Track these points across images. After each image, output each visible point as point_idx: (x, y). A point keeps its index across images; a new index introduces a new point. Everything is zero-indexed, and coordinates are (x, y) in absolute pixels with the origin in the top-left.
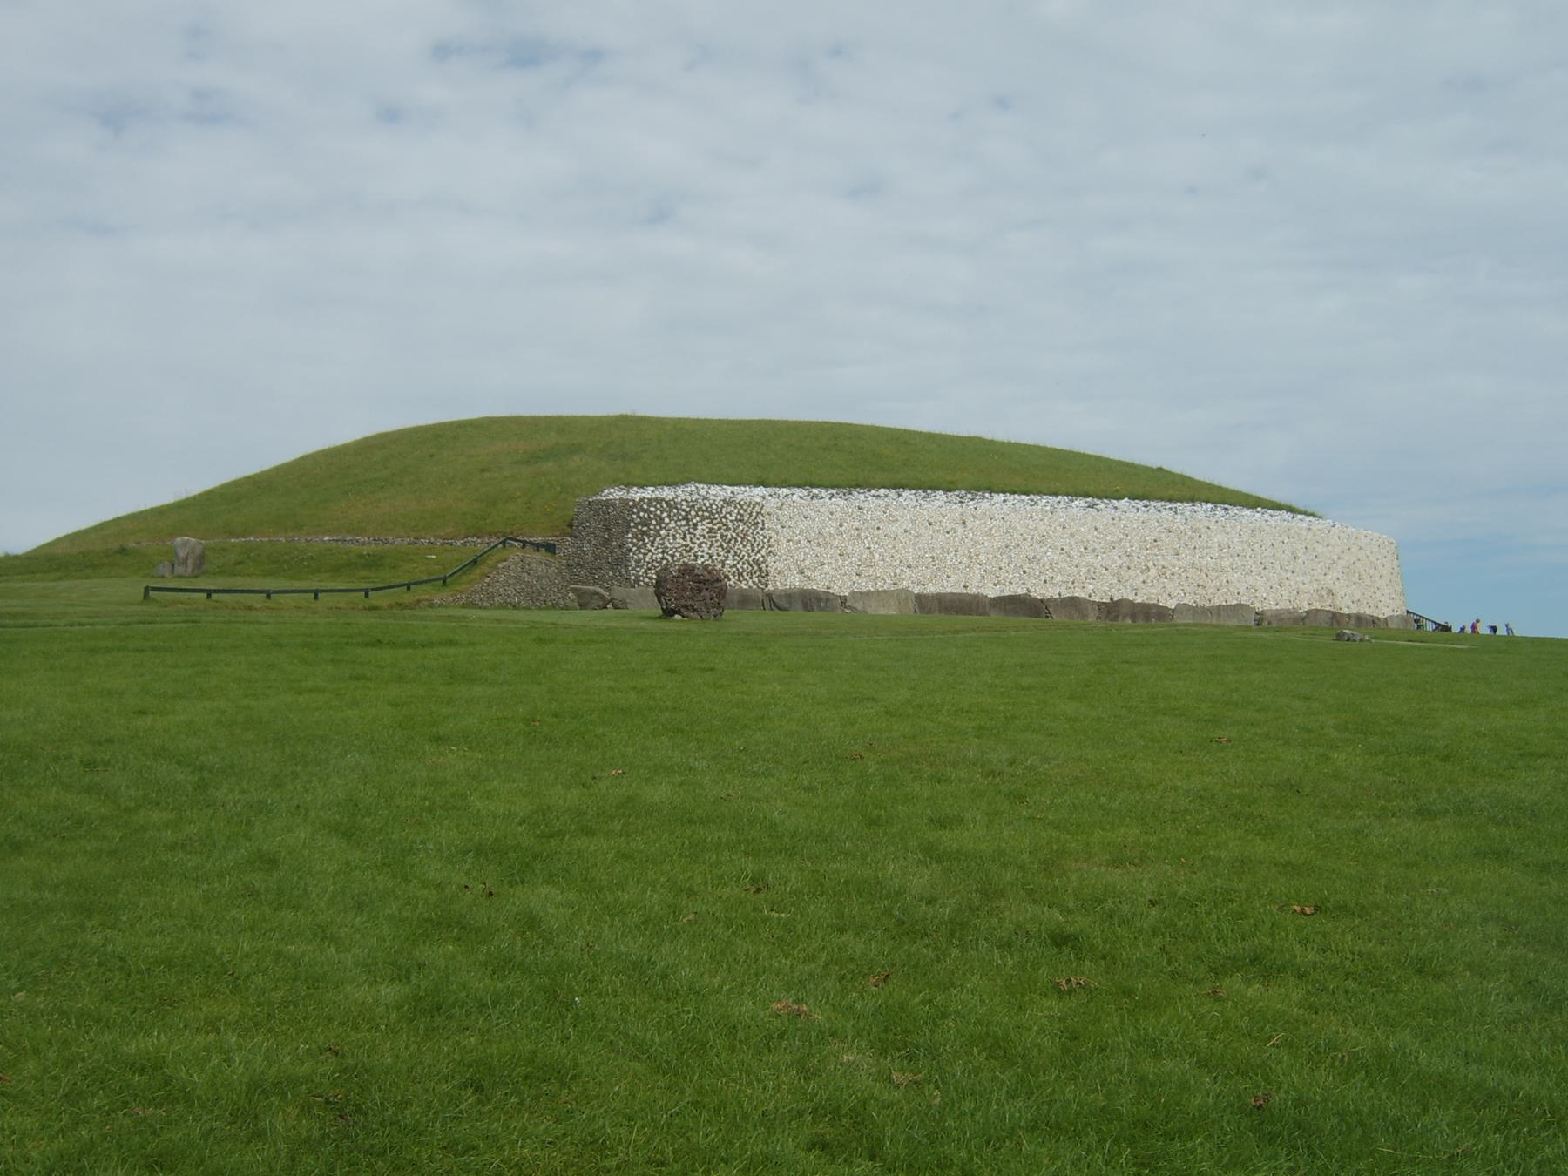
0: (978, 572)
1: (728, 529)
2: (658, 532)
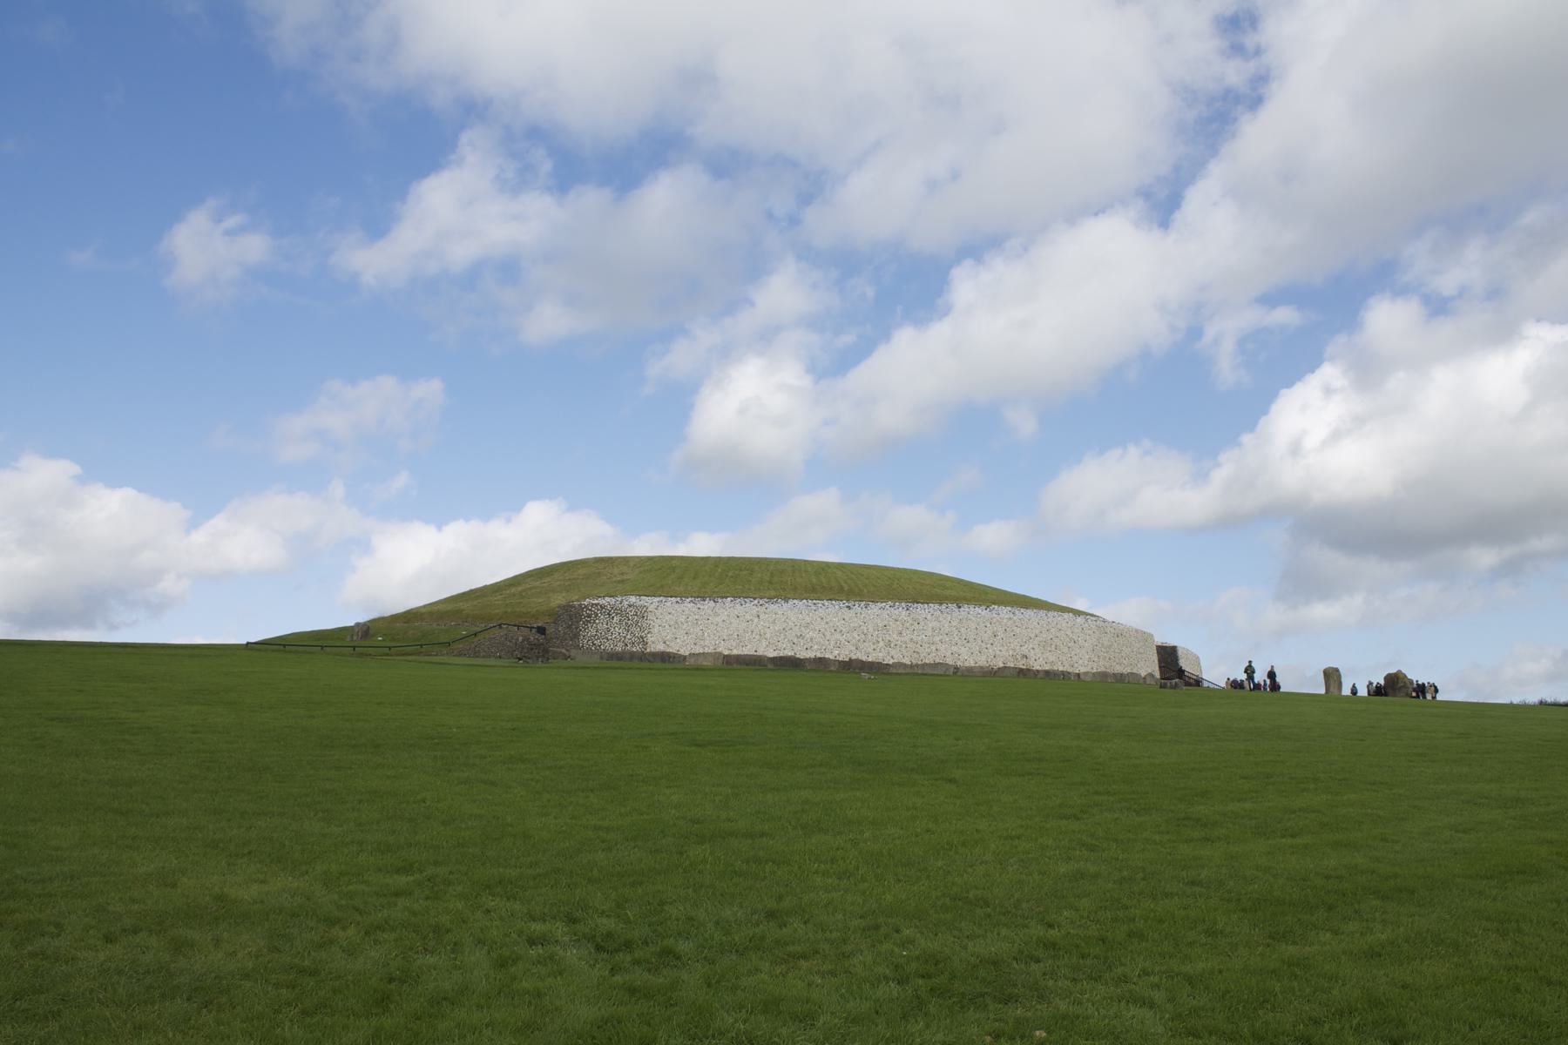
0: (764, 643)
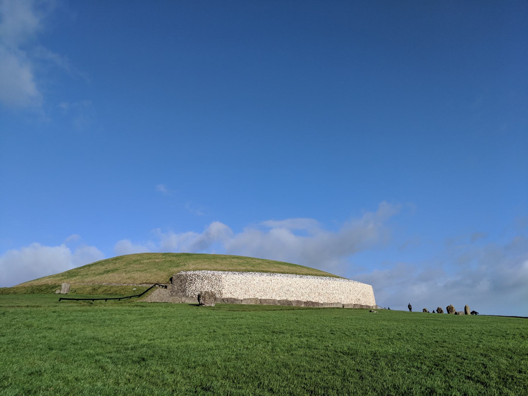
0: (275, 294)
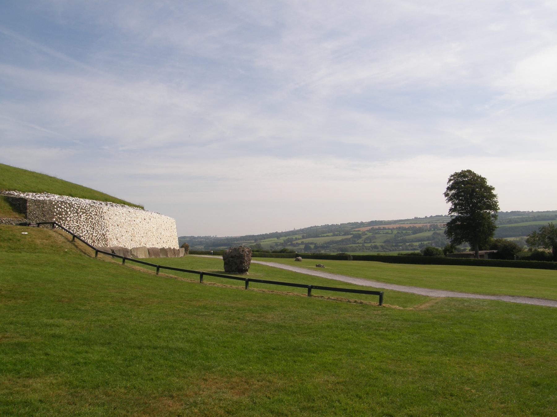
1: (92, 219)
2: (66, 218)
